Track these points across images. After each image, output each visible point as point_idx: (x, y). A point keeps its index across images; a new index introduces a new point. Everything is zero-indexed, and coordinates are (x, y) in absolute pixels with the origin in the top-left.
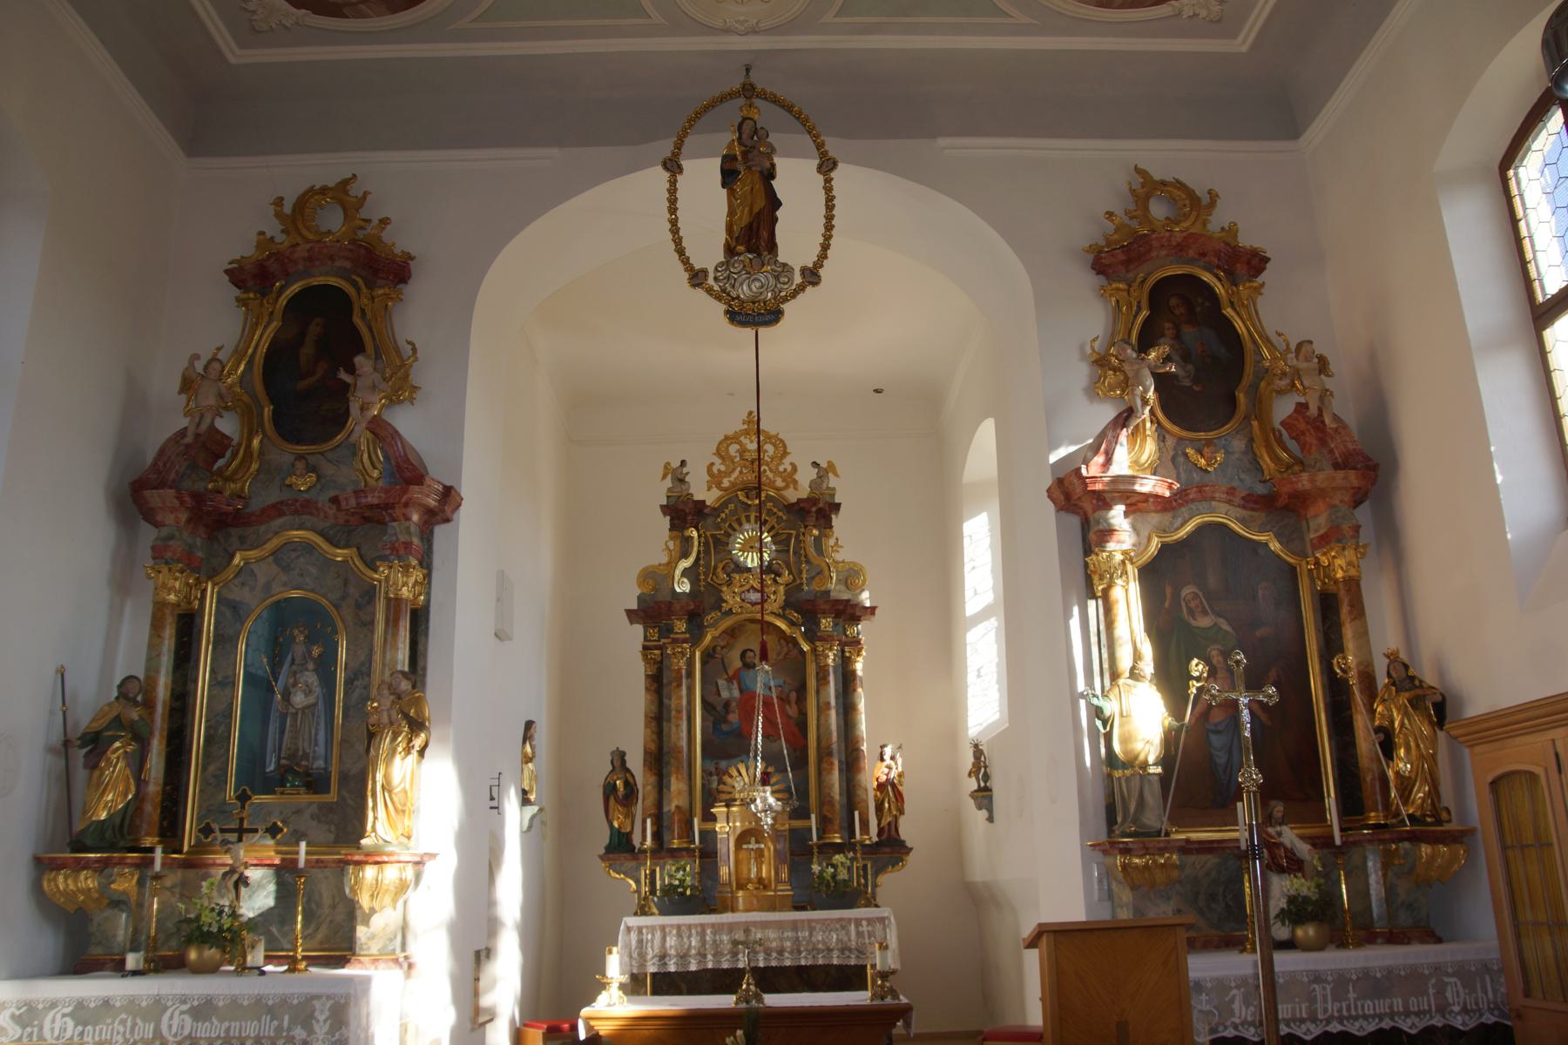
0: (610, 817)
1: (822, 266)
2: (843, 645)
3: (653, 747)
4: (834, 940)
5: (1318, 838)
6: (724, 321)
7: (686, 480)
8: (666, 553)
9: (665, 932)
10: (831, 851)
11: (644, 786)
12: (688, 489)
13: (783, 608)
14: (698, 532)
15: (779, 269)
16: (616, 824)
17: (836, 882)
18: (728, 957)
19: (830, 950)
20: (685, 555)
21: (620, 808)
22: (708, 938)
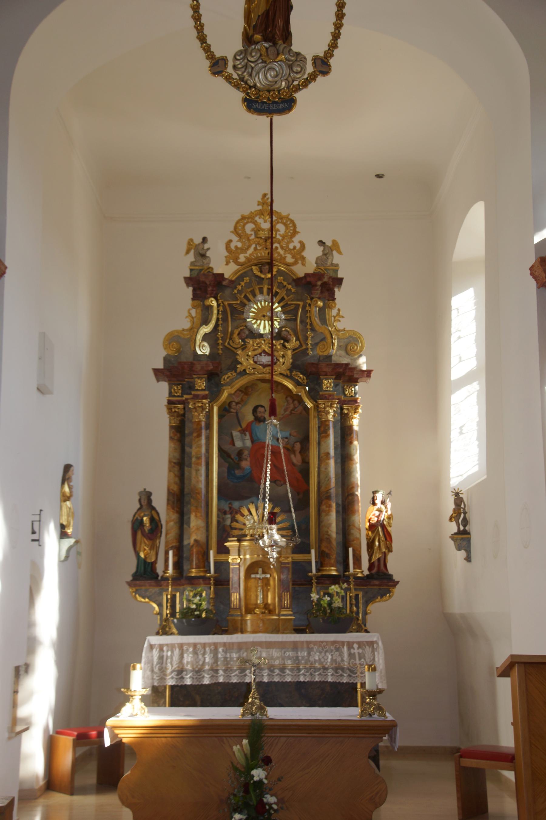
0: (138, 549)
1: (332, 56)
2: (342, 403)
3: (175, 488)
4: (329, 660)
6: (242, 108)
7: (208, 254)
8: (188, 319)
9: (183, 650)
10: (328, 582)
11: (167, 523)
12: (209, 263)
13: (291, 370)
14: (217, 300)
15: (293, 58)
16: (142, 555)
17: (331, 609)
18: (237, 672)
19: (325, 669)
20: (206, 322)
21: (146, 542)
22: (220, 656)
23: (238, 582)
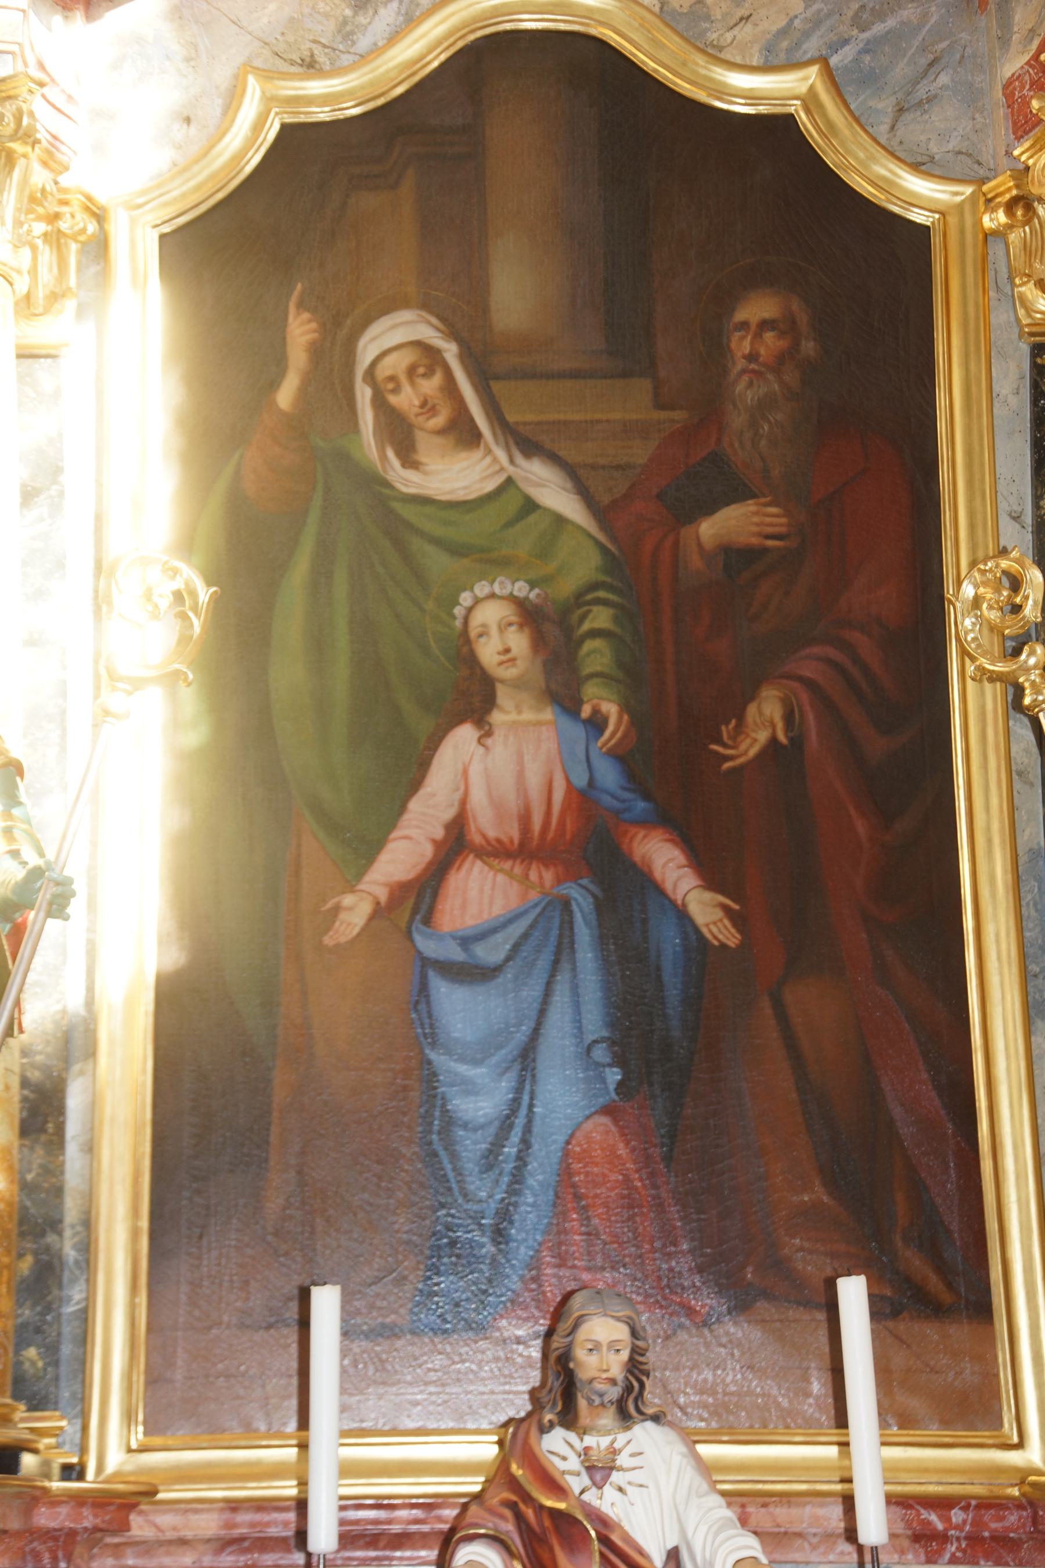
5: (942, 1504)
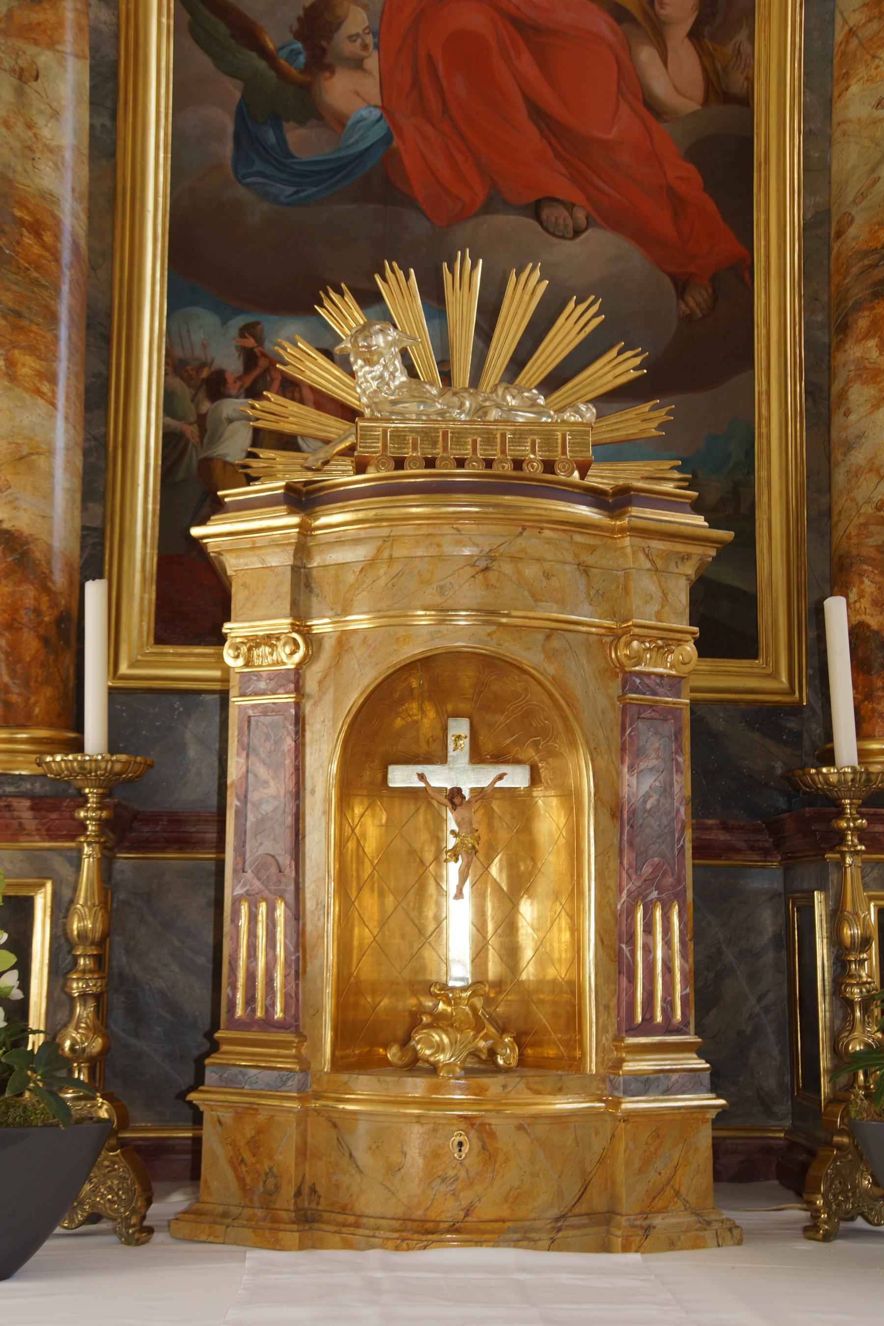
23: (290, 820)
